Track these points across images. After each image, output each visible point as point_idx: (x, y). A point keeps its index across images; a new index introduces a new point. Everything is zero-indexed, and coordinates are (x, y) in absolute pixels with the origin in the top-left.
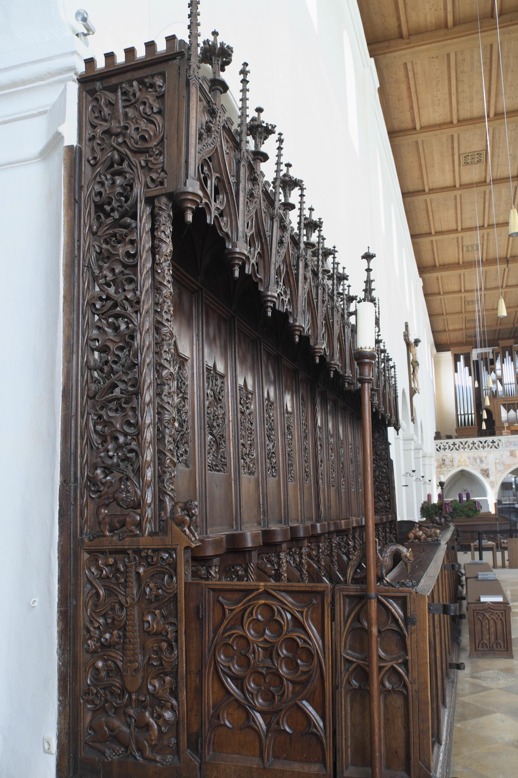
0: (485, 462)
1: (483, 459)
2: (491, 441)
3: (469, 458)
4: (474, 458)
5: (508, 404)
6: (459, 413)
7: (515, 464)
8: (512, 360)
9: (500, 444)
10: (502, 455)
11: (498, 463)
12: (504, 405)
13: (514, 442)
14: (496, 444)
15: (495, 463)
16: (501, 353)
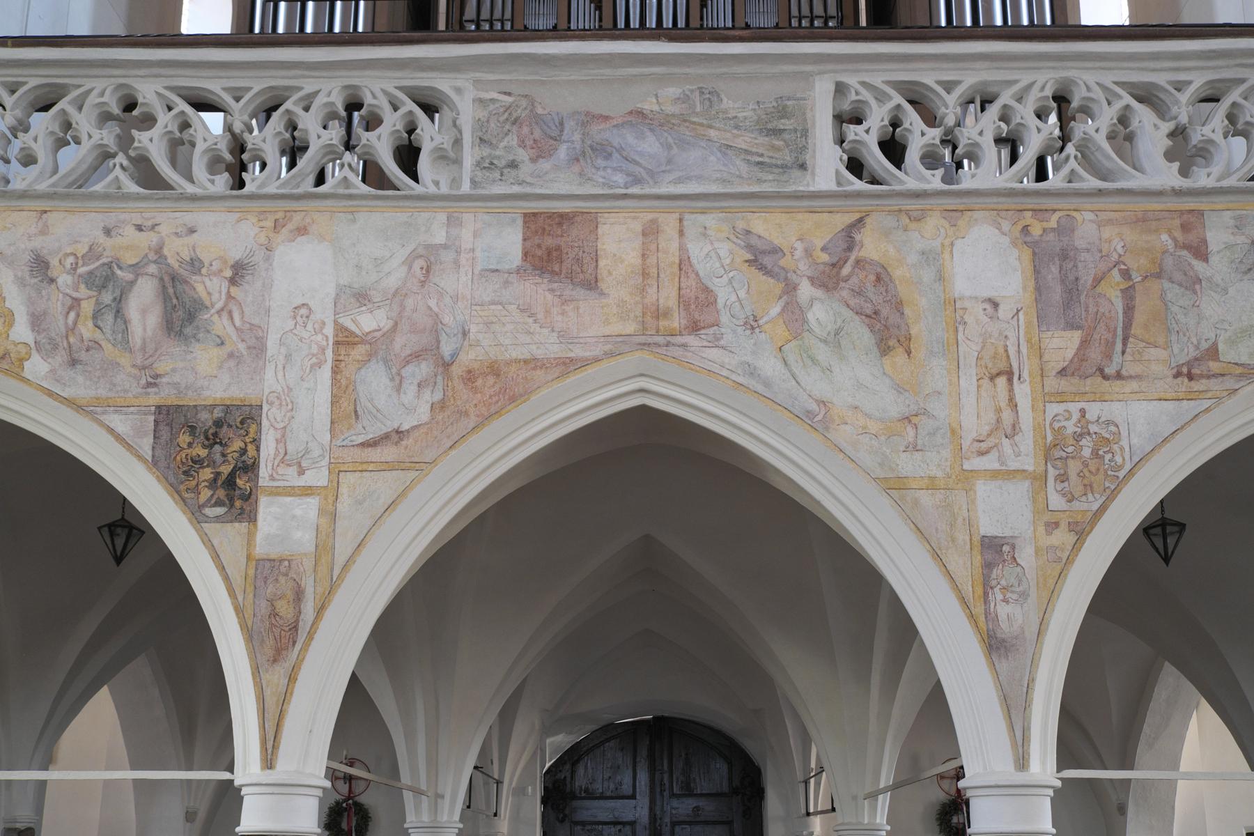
0: (221, 325)
1: (210, 288)
3: (40, 265)
7: (568, 365)
9: (430, 135)
11: (374, 346)
13: (588, 119)
15: (345, 340)
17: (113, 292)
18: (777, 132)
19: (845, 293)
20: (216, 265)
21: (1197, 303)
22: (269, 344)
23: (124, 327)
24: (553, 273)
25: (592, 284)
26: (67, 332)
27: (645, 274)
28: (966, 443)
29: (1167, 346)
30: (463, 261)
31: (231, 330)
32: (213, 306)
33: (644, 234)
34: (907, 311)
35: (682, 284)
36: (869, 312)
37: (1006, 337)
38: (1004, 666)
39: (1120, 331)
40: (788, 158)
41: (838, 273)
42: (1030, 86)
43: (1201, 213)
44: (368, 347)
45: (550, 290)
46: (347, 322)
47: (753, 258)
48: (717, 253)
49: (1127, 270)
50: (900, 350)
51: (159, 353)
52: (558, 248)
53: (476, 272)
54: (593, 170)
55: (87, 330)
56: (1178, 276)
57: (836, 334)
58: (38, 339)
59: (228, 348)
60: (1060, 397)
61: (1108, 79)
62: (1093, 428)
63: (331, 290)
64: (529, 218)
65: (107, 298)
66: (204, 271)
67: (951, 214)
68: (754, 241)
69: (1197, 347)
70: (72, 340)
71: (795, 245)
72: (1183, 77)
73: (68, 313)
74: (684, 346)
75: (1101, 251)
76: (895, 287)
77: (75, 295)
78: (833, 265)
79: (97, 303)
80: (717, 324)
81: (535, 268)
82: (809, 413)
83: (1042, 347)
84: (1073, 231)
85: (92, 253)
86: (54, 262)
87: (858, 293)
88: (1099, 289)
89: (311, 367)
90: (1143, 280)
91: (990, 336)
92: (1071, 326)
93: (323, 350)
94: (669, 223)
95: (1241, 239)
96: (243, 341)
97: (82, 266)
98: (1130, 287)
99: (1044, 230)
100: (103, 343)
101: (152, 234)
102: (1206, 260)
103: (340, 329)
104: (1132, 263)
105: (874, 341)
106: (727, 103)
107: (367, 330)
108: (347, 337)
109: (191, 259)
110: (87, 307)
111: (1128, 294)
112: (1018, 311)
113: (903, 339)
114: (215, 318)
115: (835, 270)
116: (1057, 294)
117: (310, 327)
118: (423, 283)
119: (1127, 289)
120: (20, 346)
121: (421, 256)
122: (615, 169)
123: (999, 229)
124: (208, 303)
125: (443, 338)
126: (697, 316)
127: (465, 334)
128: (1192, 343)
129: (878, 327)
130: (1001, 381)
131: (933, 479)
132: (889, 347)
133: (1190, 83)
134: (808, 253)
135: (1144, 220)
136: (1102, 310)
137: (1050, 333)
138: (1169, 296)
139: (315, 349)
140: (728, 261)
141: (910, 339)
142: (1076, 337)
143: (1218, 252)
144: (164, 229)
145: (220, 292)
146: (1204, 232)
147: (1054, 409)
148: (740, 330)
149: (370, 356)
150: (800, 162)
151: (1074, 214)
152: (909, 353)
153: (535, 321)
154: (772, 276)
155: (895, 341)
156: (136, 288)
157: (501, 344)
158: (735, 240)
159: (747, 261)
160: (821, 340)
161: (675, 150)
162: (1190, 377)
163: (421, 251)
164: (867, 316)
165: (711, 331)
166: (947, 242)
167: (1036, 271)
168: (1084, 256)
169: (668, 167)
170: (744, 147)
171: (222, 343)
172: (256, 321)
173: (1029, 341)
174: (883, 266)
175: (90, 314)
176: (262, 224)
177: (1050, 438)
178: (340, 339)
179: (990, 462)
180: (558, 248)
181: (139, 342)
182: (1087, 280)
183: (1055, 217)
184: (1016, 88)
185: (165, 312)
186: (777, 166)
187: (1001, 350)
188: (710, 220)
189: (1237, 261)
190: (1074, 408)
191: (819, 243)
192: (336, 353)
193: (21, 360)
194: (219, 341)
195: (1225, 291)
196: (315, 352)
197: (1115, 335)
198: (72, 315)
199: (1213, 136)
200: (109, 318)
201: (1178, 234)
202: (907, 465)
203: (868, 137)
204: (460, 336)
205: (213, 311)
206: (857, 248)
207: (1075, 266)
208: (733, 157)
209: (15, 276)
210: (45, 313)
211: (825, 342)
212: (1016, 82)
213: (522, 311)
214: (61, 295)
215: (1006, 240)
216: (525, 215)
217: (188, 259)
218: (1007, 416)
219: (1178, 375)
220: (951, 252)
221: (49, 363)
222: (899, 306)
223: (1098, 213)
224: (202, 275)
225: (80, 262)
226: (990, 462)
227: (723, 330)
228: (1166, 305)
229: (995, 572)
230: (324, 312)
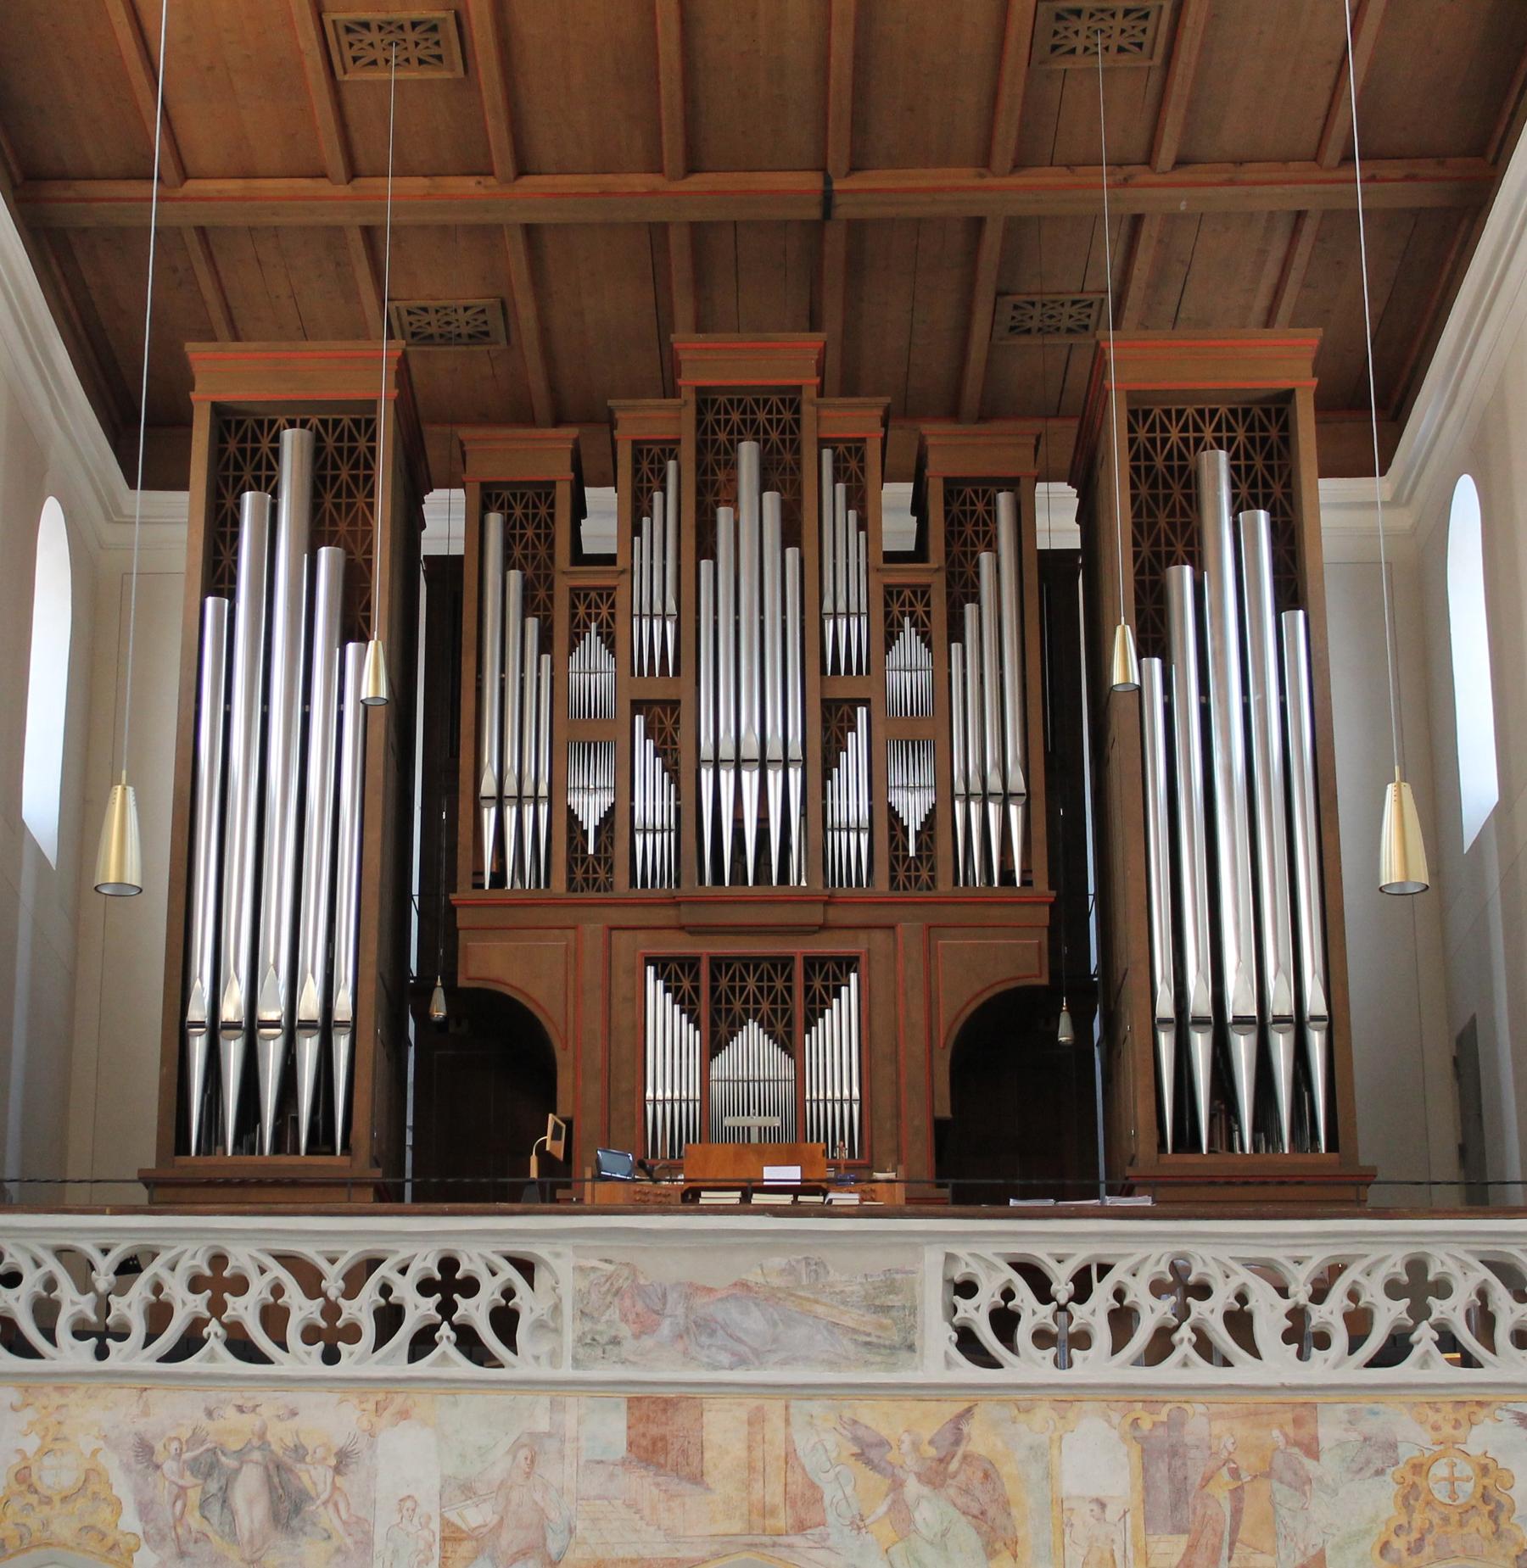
0: (328, 1519)
1: (315, 1477)
2: (427, 1264)
3: (145, 1450)
4: (208, 1466)
5: (717, 964)
6: (198, 1011)
8: (791, 535)
10: (532, 1451)
12: (674, 972)
13: (693, 1290)
14: (475, 1311)
15: (452, 1536)
16: (688, 450)
17: (219, 1481)
18: (886, 1309)
19: (952, 1492)
20: (320, 1453)
21: (1306, 1506)
22: (377, 1539)
23: (231, 1518)
24: (660, 1466)
25: (698, 1478)
26: (175, 1523)
27: (751, 1468)
29: (1274, 1551)
30: (569, 1449)
31: (336, 1522)
32: (318, 1496)
33: (750, 1423)
34: (1014, 1511)
35: (789, 1480)
36: (976, 1512)
37: (1113, 1540)
39: (1227, 1537)
40: (897, 1339)
41: (946, 1469)
42: (1146, 1259)
43: (1314, 1406)
44: (474, 1543)
45: (657, 1485)
46: (453, 1516)
47: (859, 1451)
48: (823, 1445)
49: (1237, 1469)
50: (1007, 1554)
51: (266, 1546)
52: (663, 1438)
53: (581, 1463)
54: (698, 1349)
55: (194, 1520)
56: (1288, 1476)
57: (943, 1536)
58: (147, 1528)
59: (335, 1542)
61: (1225, 1254)
63: (437, 1483)
64: (634, 1402)
65: (213, 1486)
66: (308, 1459)
67: (1059, 1404)
68: (861, 1432)
69: (1304, 1554)
70: (180, 1530)
71: (903, 1438)
72: (1300, 1253)
73: (174, 1503)
74: (790, 1546)
75: (1210, 1448)
76: (1003, 1485)
77: (181, 1482)
78: (941, 1461)
79: (204, 1492)
80: (823, 1524)
81: (640, 1460)
83: (1149, 1551)
84: (1183, 1425)
85: (196, 1438)
86: (159, 1447)
87: (966, 1491)
88: (1207, 1490)
89: (419, 1563)
90: (1252, 1480)
91: (1097, 1540)
92: (1179, 1530)
93: (430, 1547)
94: (775, 1408)
96: (350, 1535)
97: (187, 1451)
98: (1239, 1487)
99: (1154, 1424)
100: (211, 1535)
101: (253, 1415)
103: (446, 1523)
105: (980, 1544)
107: (474, 1525)
108: (453, 1532)
109: (295, 1446)
110: (194, 1496)
111: (1237, 1494)
112: (1125, 1513)
113: (1009, 1542)
114: (321, 1509)
115: (943, 1465)
116: (1165, 1493)
117: (416, 1520)
118: (528, 1475)
119: (1236, 1489)
120: (129, 1536)
121: (526, 1446)
122: (720, 1348)
123: (1109, 1421)
124: (313, 1493)
125: (550, 1536)
126: (803, 1516)
127: (571, 1531)
128: (1299, 1549)
129: (984, 1529)
132: (995, 1550)
133: (1310, 1258)
134: (916, 1446)
135: (1256, 1414)
136: (1209, 1512)
137: (1156, 1537)
138: (1278, 1498)
139: (422, 1545)
140: (833, 1455)
141: (1017, 1542)
142: (1183, 1541)
143: (1330, 1450)
144: (266, 1411)
145: (325, 1483)
146: (1316, 1426)
148: (846, 1530)
149: (477, 1553)
150: (908, 1342)
151: (1185, 1406)
152: (1015, 1557)
153: (642, 1518)
154: (879, 1472)
155: (1002, 1544)
156: (241, 1477)
157: (608, 1543)
158: (842, 1430)
159: (853, 1455)
160: (927, 1541)
161: (781, 1327)
163: (525, 1440)
164: (975, 1517)
165: (817, 1531)
166: (1056, 1436)
167: (1145, 1469)
168: (1193, 1453)
169: (774, 1346)
170: (851, 1324)
171: (329, 1537)
172: (362, 1514)
173: (1135, 1545)
174: (991, 1462)
175: (197, 1503)
176: (364, 1406)
178: (447, 1535)
180: (663, 1438)
181: (246, 1535)
182: (1196, 1479)
183: (1166, 1409)
184: (1131, 1261)
185: (272, 1502)
186: (885, 1346)
187: (1107, 1555)
188: (816, 1407)
189: (1349, 1459)
191: (927, 1435)
192: (443, 1548)
193: (130, 1552)
194: (326, 1535)
195: (1335, 1492)
196: (422, 1548)
197: (1221, 1539)
198: (179, 1504)
199: (1330, 1319)
200: (216, 1507)
201: (1290, 1430)
203: (977, 1313)
204: (566, 1533)
205: (319, 1502)
206: (964, 1442)
207: (1185, 1464)
208: (841, 1337)
209: (121, 1461)
210: (152, 1502)
211: (932, 1544)
212: (1131, 1255)
213: (629, 1506)
214: (167, 1483)
215: (1115, 1434)
216: (630, 1400)
217: (292, 1445)
220: (1060, 1447)
221: (159, 1555)
222: (1005, 1505)
223: (1209, 1405)
224: (306, 1463)
225: (184, 1449)
227: (829, 1530)
228: (1274, 1507)
230: (429, 1505)
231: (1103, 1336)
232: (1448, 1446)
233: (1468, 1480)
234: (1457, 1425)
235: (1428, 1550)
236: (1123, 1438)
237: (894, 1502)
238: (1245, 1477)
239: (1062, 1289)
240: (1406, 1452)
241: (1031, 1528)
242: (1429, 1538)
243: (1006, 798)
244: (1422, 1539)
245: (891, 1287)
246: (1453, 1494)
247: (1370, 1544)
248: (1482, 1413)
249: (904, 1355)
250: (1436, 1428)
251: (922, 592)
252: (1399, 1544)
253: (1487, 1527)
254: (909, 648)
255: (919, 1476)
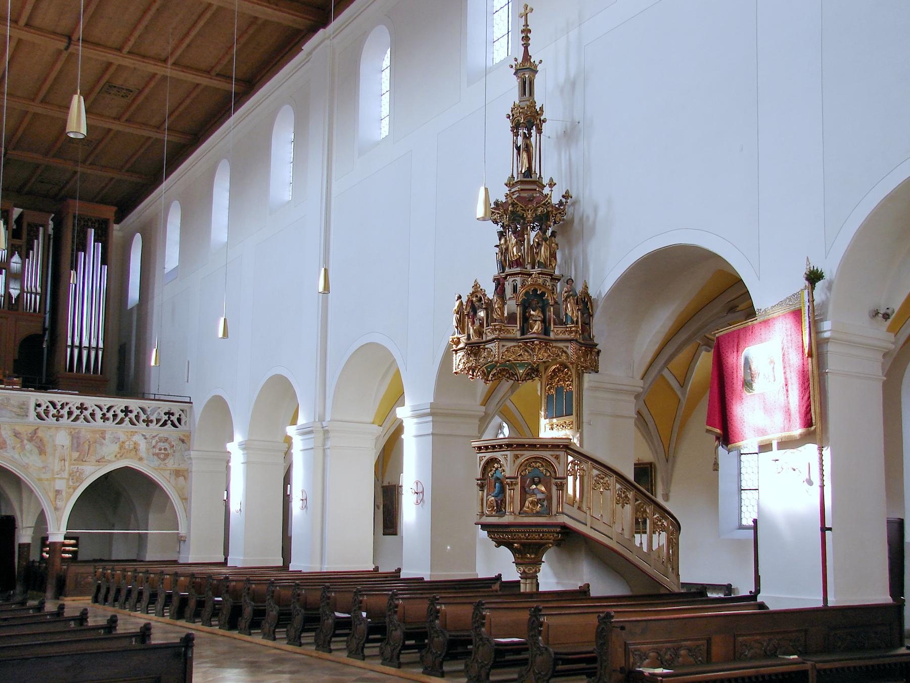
18: (22, 408)
19: (34, 443)
28: (55, 472)
34: (46, 447)
38: (57, 513)
42: (75, 403)
43: (105, 431)
60: (74, 464)
62: (80, 470)
72: (106, 404)
82: (24, 466)
87: (36, 443)
92: (78, 451)
95: (112, 437)
102: (105, 440)
104: (91, 440)
106: (12, 401)
111: (89, 446)
116: (76, 445)
130: (63, 461)
131: (47, 479)
134: (27, 434)
142: (78, 453)
147: (72, 467)
152: (45, 455)
162: (99, 462)
177: (71, 472)
179: (59, 476)
182: (82, 443)
184: (73, 403)
190: (77, 466)
191: (30, 432)
201: (101, 435)
202: (43, 476)
203: (41, 410)
215: (67, 434)
218: (63, 468)
219: (97, 461)
226: (59, 476)
229: (58, 496)
231: (66, 416)
232: (129, 439)
233: (132, 445)
234: (131, 436)
235: (123, 457)
236: (69, 435)
237: (21, 445)
238: (91, 442)
239: (59, 407)
240: (121, 440)
241: (49, 449)
242: (124, 455)
243: (36, 294)
244: (122, 455)
245: (24, 404)
246: (129, 447)
247: (113, 455)
248: (136, 434)
249: (26, 417)
250: (127, 436)
251: (20, 246)
252: (118, 455)
253: (134, 453)
254: (16, 258)
255: (27, 440)
